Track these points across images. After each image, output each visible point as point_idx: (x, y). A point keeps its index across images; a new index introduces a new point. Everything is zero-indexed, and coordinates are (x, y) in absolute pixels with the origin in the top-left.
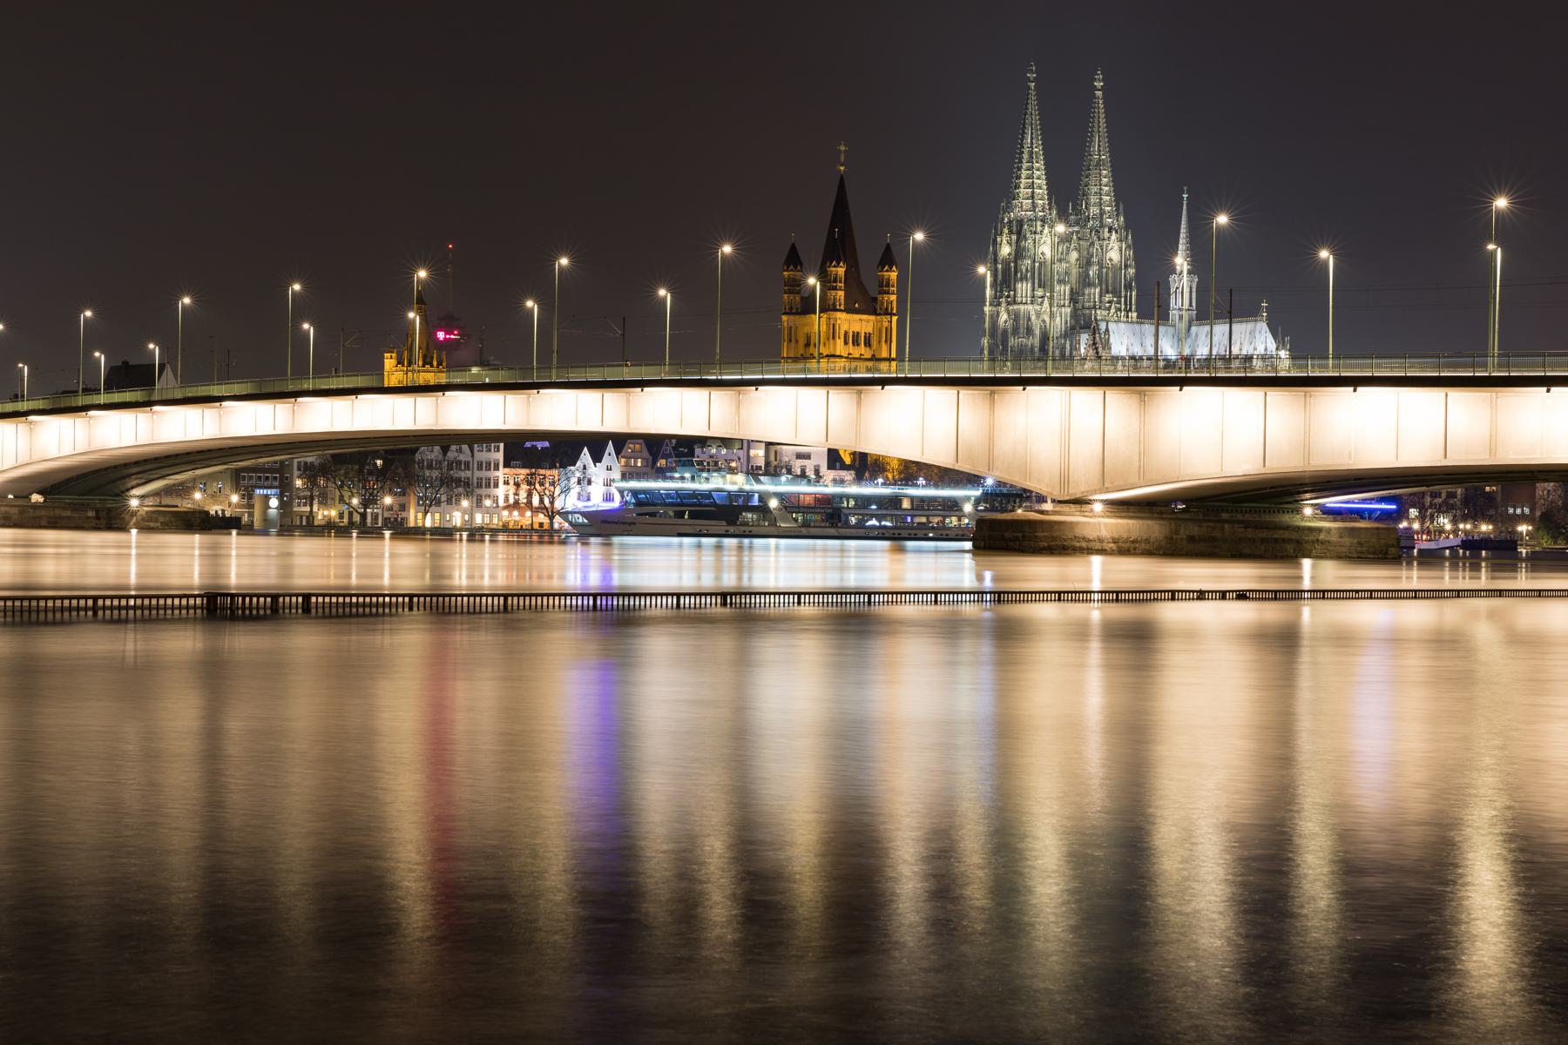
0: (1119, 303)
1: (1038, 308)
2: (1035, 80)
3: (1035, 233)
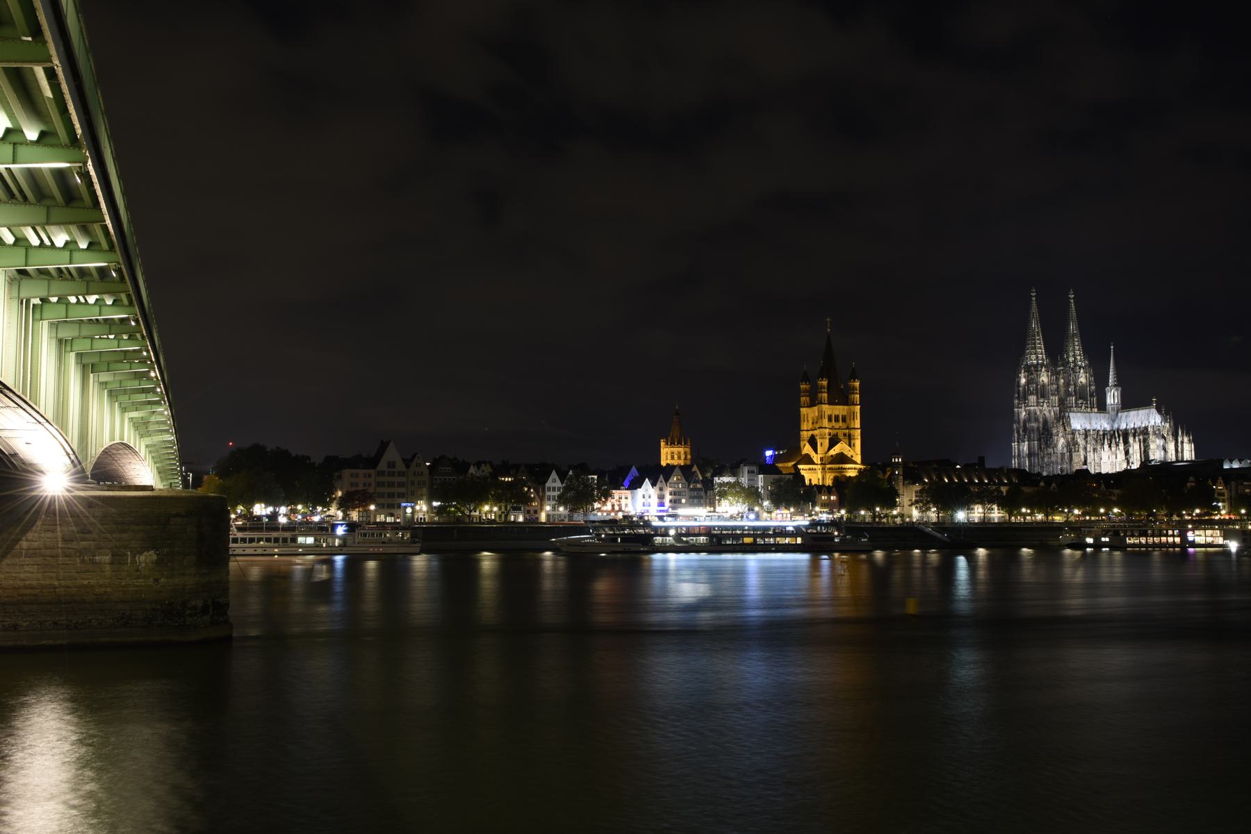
0: (1087, 403)
1: (1041, 408)
2: (1035, 296)
3: (1038, 371)
